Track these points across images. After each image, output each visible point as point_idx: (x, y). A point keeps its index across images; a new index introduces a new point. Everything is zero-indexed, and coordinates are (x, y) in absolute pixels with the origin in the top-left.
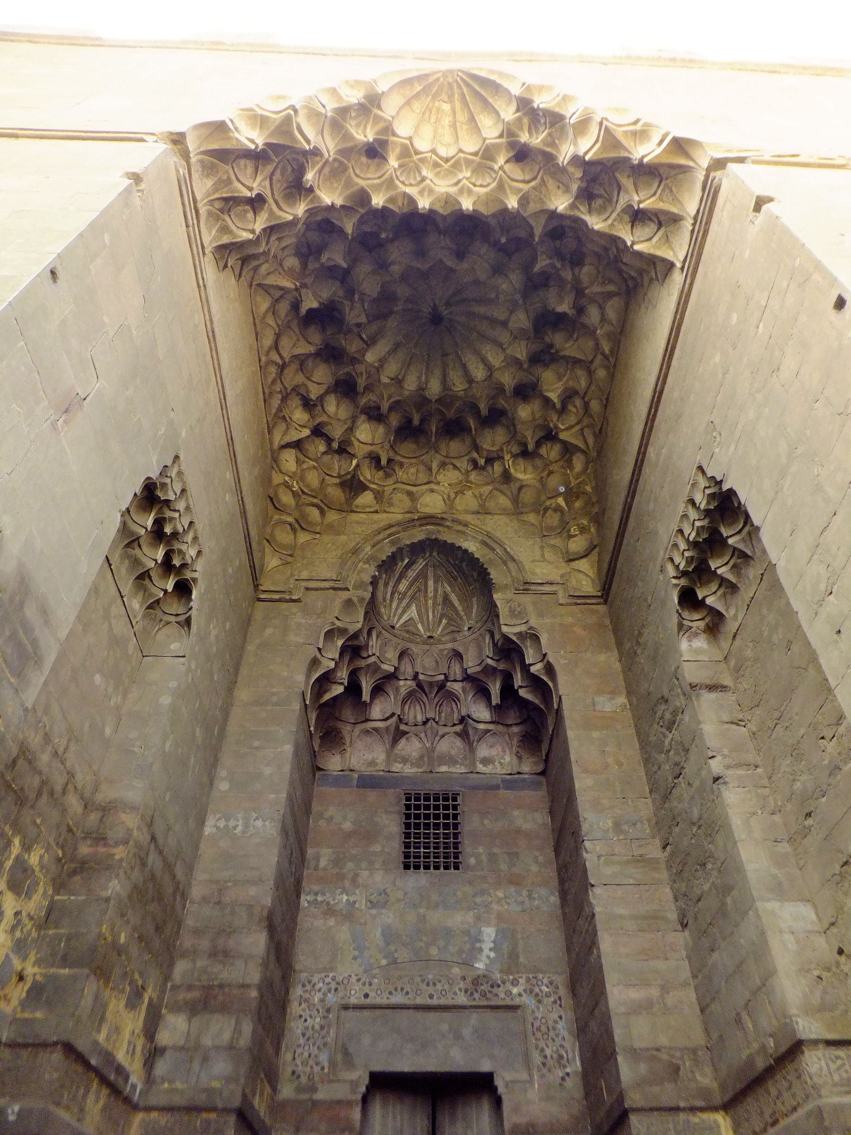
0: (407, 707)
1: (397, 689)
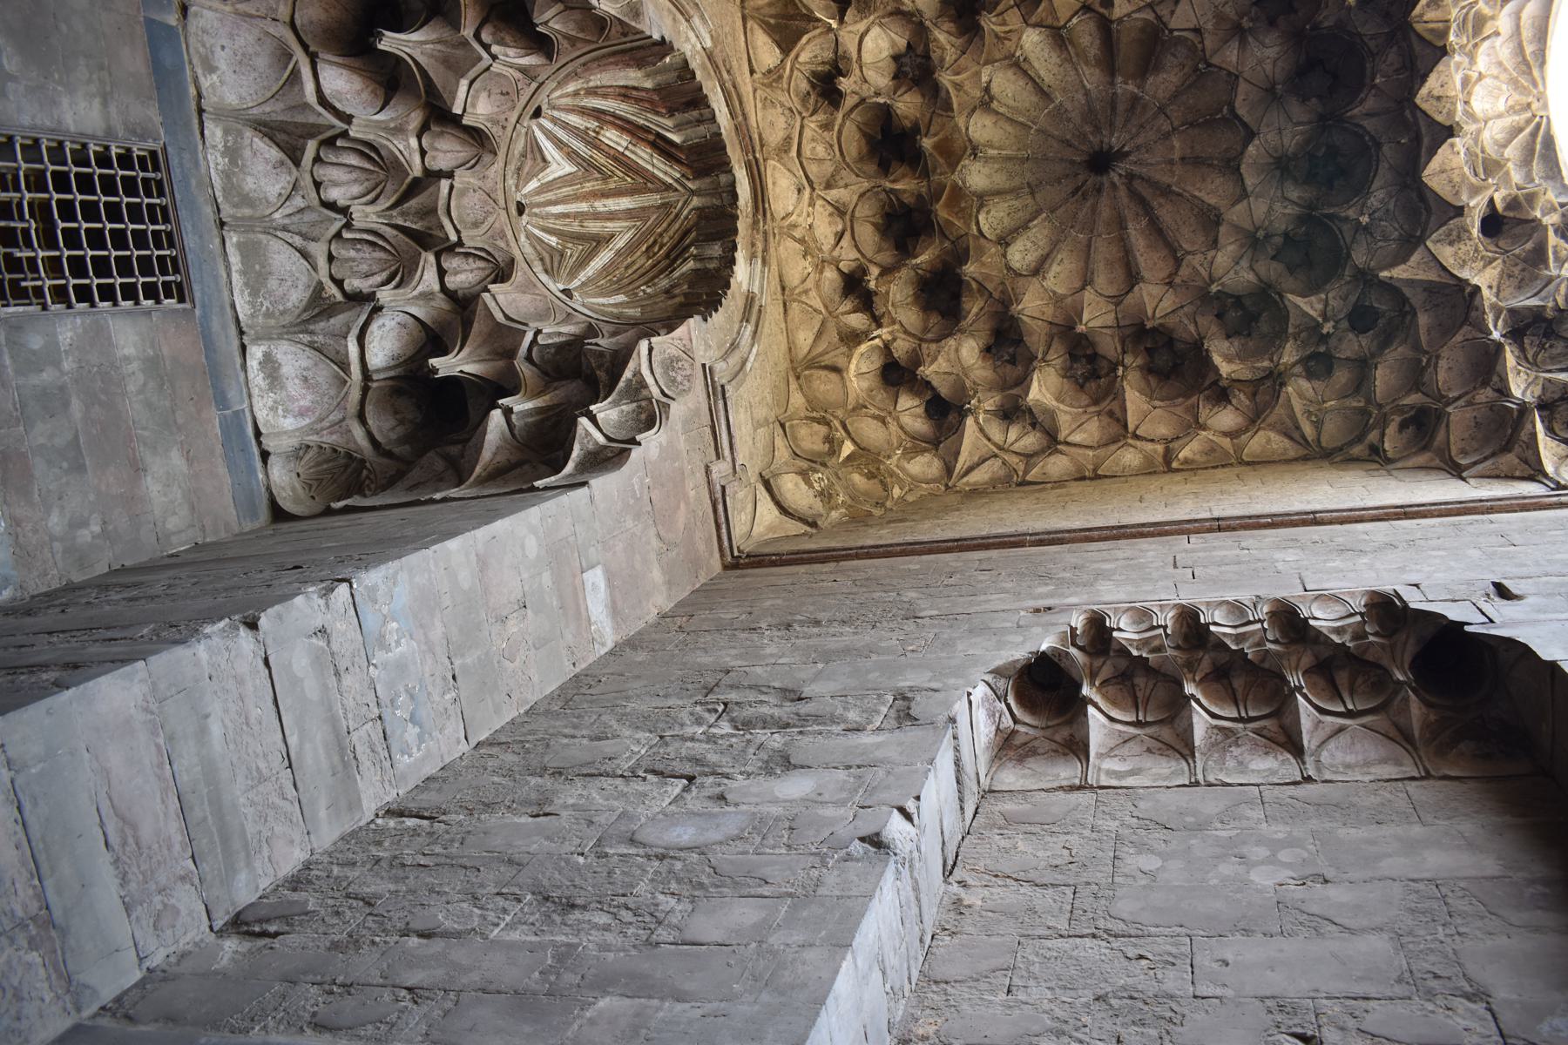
0: (353, 160)
1: (399, 130)
